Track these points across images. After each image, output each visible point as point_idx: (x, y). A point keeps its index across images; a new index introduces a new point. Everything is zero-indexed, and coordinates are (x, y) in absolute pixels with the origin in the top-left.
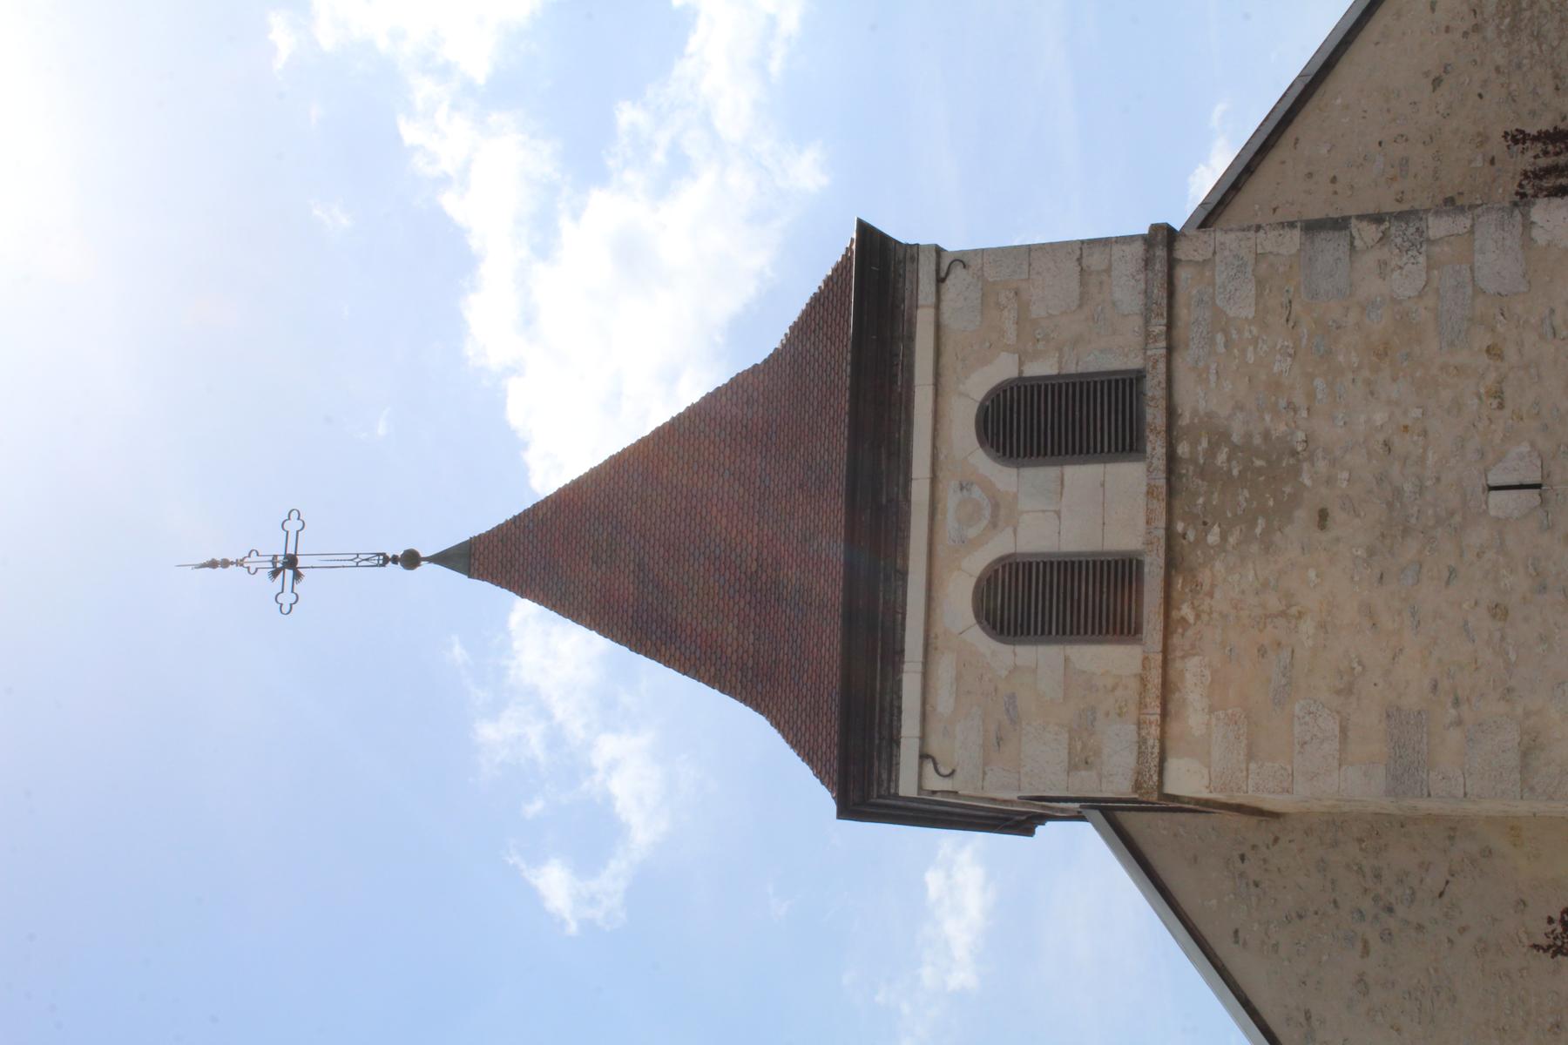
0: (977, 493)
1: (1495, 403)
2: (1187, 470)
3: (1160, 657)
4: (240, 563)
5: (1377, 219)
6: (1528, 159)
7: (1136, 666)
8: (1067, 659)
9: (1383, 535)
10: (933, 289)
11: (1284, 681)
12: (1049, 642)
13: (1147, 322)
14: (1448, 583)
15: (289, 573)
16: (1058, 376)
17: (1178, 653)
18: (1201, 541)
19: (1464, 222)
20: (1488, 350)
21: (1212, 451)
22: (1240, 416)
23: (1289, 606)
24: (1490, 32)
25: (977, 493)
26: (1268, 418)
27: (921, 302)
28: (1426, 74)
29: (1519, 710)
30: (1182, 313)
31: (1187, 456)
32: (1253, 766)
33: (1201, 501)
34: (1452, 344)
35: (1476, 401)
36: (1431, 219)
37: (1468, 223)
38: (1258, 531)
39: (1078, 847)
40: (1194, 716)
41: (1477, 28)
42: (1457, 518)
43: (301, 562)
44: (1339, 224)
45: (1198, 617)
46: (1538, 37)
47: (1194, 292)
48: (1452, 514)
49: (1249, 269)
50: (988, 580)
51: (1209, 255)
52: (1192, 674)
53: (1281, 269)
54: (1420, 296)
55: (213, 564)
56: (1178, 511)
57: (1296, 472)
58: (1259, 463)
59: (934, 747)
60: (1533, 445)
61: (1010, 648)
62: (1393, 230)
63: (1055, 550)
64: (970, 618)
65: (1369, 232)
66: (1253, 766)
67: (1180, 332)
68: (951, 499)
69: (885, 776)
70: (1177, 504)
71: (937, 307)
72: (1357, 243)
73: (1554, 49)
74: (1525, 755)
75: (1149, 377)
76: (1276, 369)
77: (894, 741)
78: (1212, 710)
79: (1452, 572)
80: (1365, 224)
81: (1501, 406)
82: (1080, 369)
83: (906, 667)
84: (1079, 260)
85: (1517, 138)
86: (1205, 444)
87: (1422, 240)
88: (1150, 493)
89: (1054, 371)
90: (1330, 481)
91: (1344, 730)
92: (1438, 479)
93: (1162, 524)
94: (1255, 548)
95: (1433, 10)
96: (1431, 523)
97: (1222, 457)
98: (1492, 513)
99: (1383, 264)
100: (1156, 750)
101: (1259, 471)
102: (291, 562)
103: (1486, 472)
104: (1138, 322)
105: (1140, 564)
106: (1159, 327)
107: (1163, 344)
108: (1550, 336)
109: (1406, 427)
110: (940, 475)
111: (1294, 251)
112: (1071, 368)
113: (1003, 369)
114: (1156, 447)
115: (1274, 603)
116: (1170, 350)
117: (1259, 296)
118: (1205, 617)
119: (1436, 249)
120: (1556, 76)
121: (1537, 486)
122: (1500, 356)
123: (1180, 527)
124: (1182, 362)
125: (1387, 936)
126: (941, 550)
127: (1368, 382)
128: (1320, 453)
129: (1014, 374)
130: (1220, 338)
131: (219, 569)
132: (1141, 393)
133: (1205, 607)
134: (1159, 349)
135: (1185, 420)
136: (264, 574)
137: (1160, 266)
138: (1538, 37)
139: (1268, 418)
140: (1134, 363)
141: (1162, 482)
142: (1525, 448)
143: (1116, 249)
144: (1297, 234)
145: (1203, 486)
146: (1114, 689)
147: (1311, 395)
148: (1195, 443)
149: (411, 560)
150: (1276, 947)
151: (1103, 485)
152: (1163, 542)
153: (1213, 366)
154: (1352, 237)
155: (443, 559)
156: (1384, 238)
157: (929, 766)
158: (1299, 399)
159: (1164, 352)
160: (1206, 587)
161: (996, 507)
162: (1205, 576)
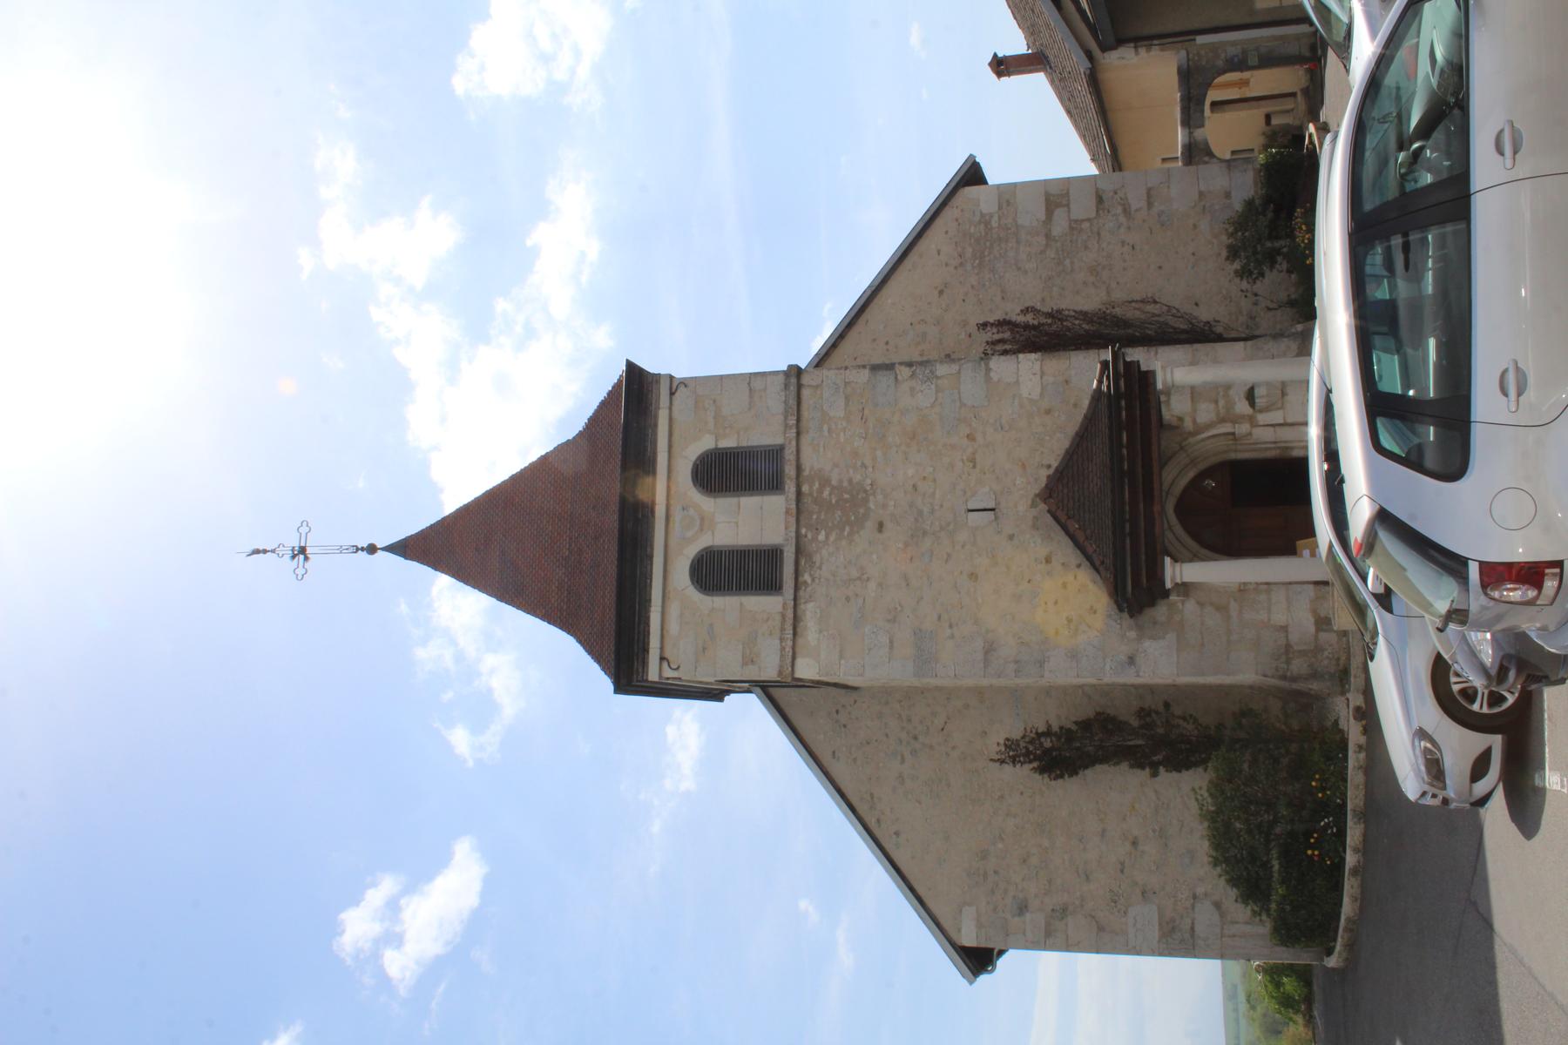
2: (807, 500)
4: (273, 551)
5: (910, 365)
7: (779, 608)
13: (786, 418)
18: (815, 539)
19: (955, 367)
21: (822, 487)
24: (969, 267)
25: (692, 511)
30: (805, 414)
39: (748, 709)
40: (811, 633)
41: (961, 264)
43: (309, 551)
44: (890, 367)
52: (810, 610)
54: (932, 406)
55: (257, 552)
56: (802, 523)
57: (866, 500)
59: (667, 654)
65: (904, 372)
67: (804, 423)
77: (646, 650)
79: (949, 555)
85: (985, 325)
87: (933, 376)
88: (787, 512)
90: (884, 506)
91: (891, 642)
93: (793, 529)
97: (826, 493)
101: (846, 501)
102: (303, 550)
105: (782, 552)
106: (792, 421)
113: (706, 443)
114: (790, 487)
115: (855, 573)
116: (798, 434)
117: (847, 404)
123: (803, 531)
124: (805, 440)
125: (914, 752)
126: (672, 543)
130: (825, 428)
132: (782, 457)
135: (806, 473)
136: (287, 558)
137: (793, 388)
140: (779, 441)
142: (987, 489)
143: (769, 378)
144: (867, 371)
145: (816, 508)
149: (372, 549)
150: (855, 760)
155: (391, 549)
156: (913, 375)
157: (665, 664)
158: (868, 462)
161: (702, 519)
162: (817, 558)
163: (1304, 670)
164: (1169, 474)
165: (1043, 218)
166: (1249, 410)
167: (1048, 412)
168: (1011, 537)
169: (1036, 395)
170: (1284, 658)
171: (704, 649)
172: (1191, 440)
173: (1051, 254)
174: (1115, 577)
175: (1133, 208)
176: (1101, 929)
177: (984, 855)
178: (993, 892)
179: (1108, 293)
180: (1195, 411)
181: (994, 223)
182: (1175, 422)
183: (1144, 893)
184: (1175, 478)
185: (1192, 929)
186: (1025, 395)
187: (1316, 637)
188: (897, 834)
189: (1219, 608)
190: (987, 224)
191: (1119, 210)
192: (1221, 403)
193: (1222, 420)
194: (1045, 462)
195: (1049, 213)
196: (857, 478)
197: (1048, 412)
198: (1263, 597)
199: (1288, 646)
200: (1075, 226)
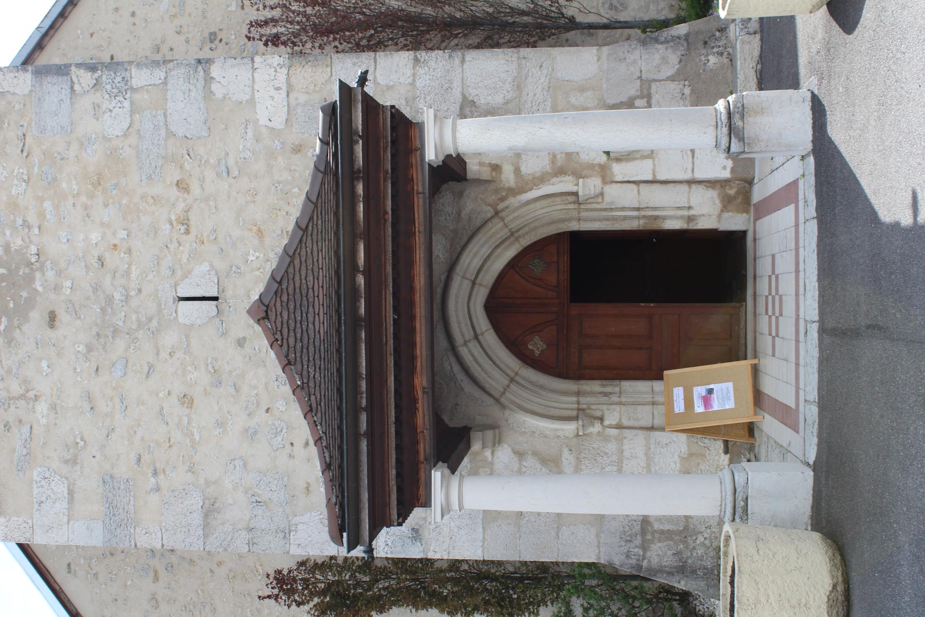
1: (183, 228)
5: (92, 68)
9: (98, 334)
11: (25, 452)
19: (159, 74)
20: (177, 185)
23: (27, 391)
29: (202, 481)
34: (150, 178)
35: (168, 226)
36: (134, 71)
37: (163, 75)
42: (154, 323)
48: (150, 320)
57: (30, 279)
60: (211, 265)
62: (104, 77)
65: (85, 79)
72: (77, 87)
74: (206, 516)
76: (14, 192)
80: (82, 71)
81: (187, 232)
90: (57, 288)
91: (71, 493)
92: (140, 291)
96: (134, 327)
98: (181, 320)
99: (96, 106)
103: (176, 285)
108: (225, 174)
109: (115, 246)
111: (26, 91)
115: (16, 388)
119: (137, 96)
121: (216, 299)
125: (170, 567)
127: (86, 208)
139: (8, 233)
142: (205, 267)
147: (42, 215)
154: (73, 82)
156: (97, 84)
158: (32, 219)
163: (669, 560)
164: (471, 260)
169: (278, 122)
170: (638, 541)
172: (513, 201)
182: (486, 174)
184: (487, 259)
186: (263, 121)
196: (17, 243)
198: (611, 447)
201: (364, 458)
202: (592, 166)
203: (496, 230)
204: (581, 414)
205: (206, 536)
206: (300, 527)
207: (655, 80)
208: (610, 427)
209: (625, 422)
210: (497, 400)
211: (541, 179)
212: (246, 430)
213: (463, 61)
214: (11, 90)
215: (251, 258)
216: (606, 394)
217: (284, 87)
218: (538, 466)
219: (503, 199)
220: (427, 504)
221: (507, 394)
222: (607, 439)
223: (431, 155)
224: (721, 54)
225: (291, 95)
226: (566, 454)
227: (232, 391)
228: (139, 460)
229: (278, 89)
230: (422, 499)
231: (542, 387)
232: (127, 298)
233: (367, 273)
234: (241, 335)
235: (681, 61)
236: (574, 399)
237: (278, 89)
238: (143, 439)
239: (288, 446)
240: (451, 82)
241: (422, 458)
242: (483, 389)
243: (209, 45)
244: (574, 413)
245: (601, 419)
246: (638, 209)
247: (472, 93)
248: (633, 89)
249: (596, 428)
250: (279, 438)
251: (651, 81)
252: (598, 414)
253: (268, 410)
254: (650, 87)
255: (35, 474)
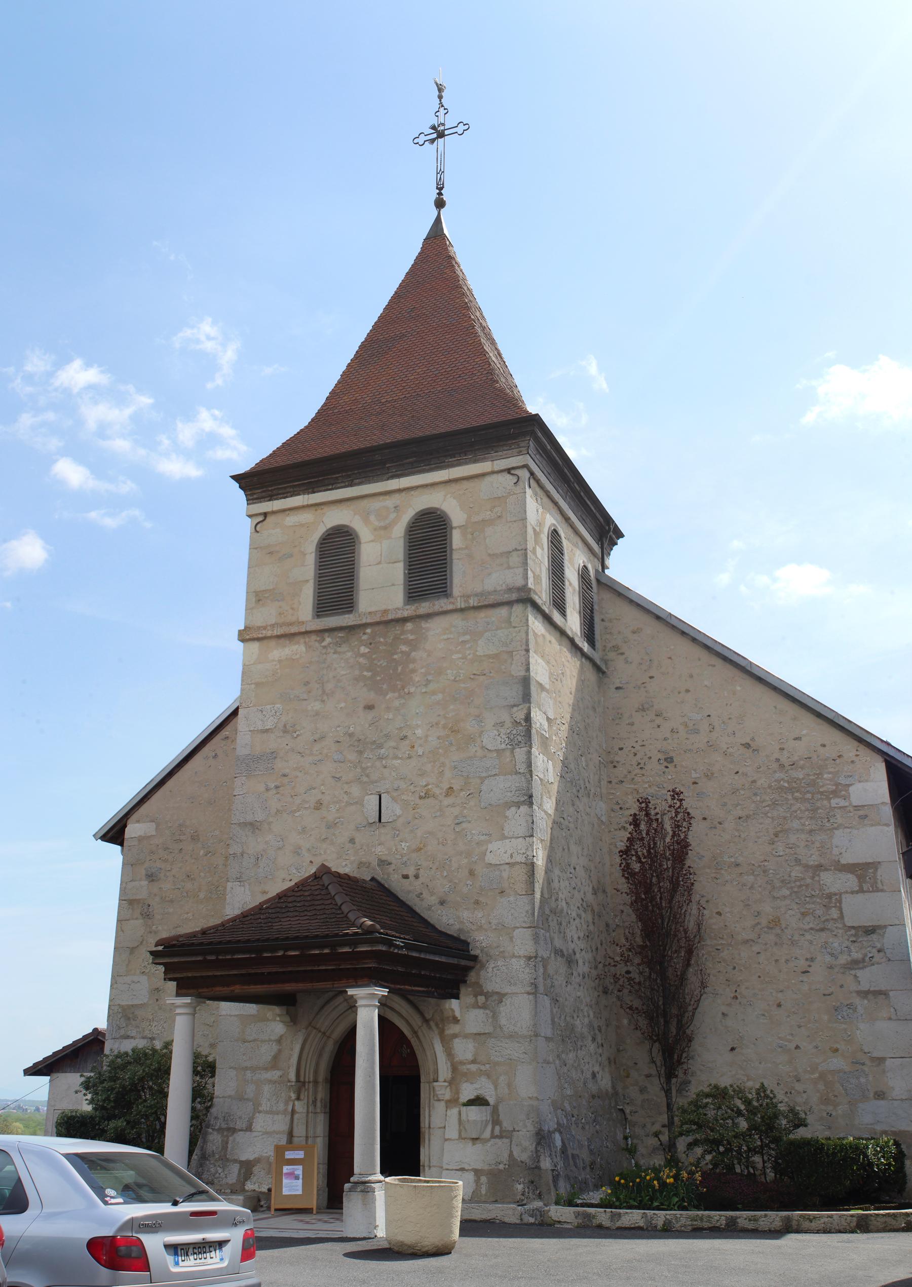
0: (393, 516)
1: (423, 794)
2: (397, 630)
3: (303, 630)
6: (660, 804)
8: (307, 581)
10: (502, 468)
12: (315, 570)
13: (476, 595)
14: (334, 777)
15: (435, 136)
16: (452, 550)
17: (307, 640)
20: (451, 788)
22: (425, 655)
25: (393, 516)
26: (423, 670)
27: (495, 462)
28: (753, 739)
29: (271, 819)
30: (482, 614)
31: (406, 628)
32: (253, 686)
33: (382, 640)
34: (455, 768)
38: (365, 673)
41: (782, 766)
42: (365, 779)
45: (324, 647)
46: (774, 804)
47: (493, 619)
48: (367, 776)
49: (504, 649)
50: (347, 532)
51: (513, 625)
52: (297, 649)
53: (503, 667)
54: (483, 747)
56: (377, 628)
58: (400, 669)
59: (270, 519)
60: (400, 816)
61: (314, 550)
62: (521, 728)
63: (362, 565)
64: (329, 526)
65: (520, 716)
66: (253, 686)
67: (472, 614)
68: (390, 502)
69: (255, 496)
70: (381, 627)
71: (493, 472)
72: (515, 709)
73: (766, 814)
74: (251, 824)
75: (445, 600)
77: (271, 498)
78: (280, 661)
81: (421, 798)
82: (454, 561)
83: (306, 496)
84: (516, 550)
86: (411, 637)
88: (386, 611)
89: (454, 547)
90: (388, 709)
91: (267, 731)
92: (385, 767)
93: (369, 621)
94: (357, 672)
95: (796, 739)
96: (363, 765)
97: (404, 648)
98: (367, 797)
99: (502, 724)
100: (260, 636)
103: (388, 792)
104: (479, 589)
105: (351, 612)
106: (473, 602)
107: (463, 606)
109: (413, 747)
110: (403, 494)
111: (513, 673)
112: (455, 556)
113: (457, 515)
114: (409, 611)
115: (329, 687)
116: (462, 610)
118: (324, 651)
119: (508, 753)
120: (748, 817)
122: (447, 795)
123: (369, 631)
124: (456, 619)
126: (365, 502)
128: (403, 701)
129: (455, 524)
131: (437, 93)
132: (439, 598)
133: (329, 650)
134: (460, 604)
135: (424, 625)
137: (506, 597)
138: (774, 804)
139: (423, 670)
140: (456, 591)
141: (390, 617)
142: (398, 812)
143: (521, 570)
144: (523, 673)
146: (293, 609)
147: (434, 693)
148: (412, 632)
149: (440, 204)
151: (393, 585)
152: (359, 622)
153: (452, 636)
155: (438, 221)
157: (261, 518)
158: (432, 687)
159: (459, 607)
160: (339, 649)
161: (385, 528)
162: (344, 648)
165: (843, 861)
166: (464, 1098)
167: (472, 873)
168: (352, 841)
169: (490, 858)
170: (224, 1126)
171: (271, 553)
173: (797, 872)
174: (183, 945)
175: (859, 973)
176: (132, 950)
177: (195, 838)
178: (166, 849)
179: (746, 942)
180: (466, 1036)
181: (834, 802)
183: (158, 990)
185: (128, 1037)
186: (490, 847)
187: (235, 1161)
188: (216, 756)
189: (276, 1058)
190: (835, 793)
191: (857, 955)
192: (473, 1067)
193: (454, 1068)
194: (421, 872)
195: (851, 868)
197: (472, 873)
198: (281, 1106)
199: (233, 1131)
200: (833, 899)
201: (194, 959)
202: (458, 1092)
203: (416, 1021)
204: (300, 1084)
205: (239, 824)
206: (243, 889)
207: (511, 1142)
208: (294, 1106)
209: (296, 1116)
210: (310, 1024)
211: (450, 1054)
212: (300, 848)
213: (529, 993)
214: (514, 662)
215: (403, 844)
216: (314, 1102)
217: (513, 861)
218: (273, 1054)
219: (437, 1025)
220: (178, 994)
221: (315, 1031)
222: (286, 1104)
223: (351, 992)
224: (523, 1195)
225: (507, 866)
226: (279, 1073)
227: (323, 837)
228: (285, 776)
229: (511, 856)
230: (180, 991)
231: (320, 1055)
232: (381, 758)
233: (284, 956)
234: (357, 840)
235: (522, 1162)
236: (311, 1079)
237: (511, 856)
238: (297, 777)
239: (290, 877)
240: (515, 984)
241: (200, 990)
242: (317, 1014)
243: (662, 757)
244: (302, 1079)
245: (298, 1099)
246: (429, 1127)
247: (507, 1001)
248: (507, 1125)
249: (293, 1096)
250: (294, 871)
251: (510, 1137)
252: (302, 1097)
253: (311, 862)
254: (507, 1138)
255: (278, 706)
